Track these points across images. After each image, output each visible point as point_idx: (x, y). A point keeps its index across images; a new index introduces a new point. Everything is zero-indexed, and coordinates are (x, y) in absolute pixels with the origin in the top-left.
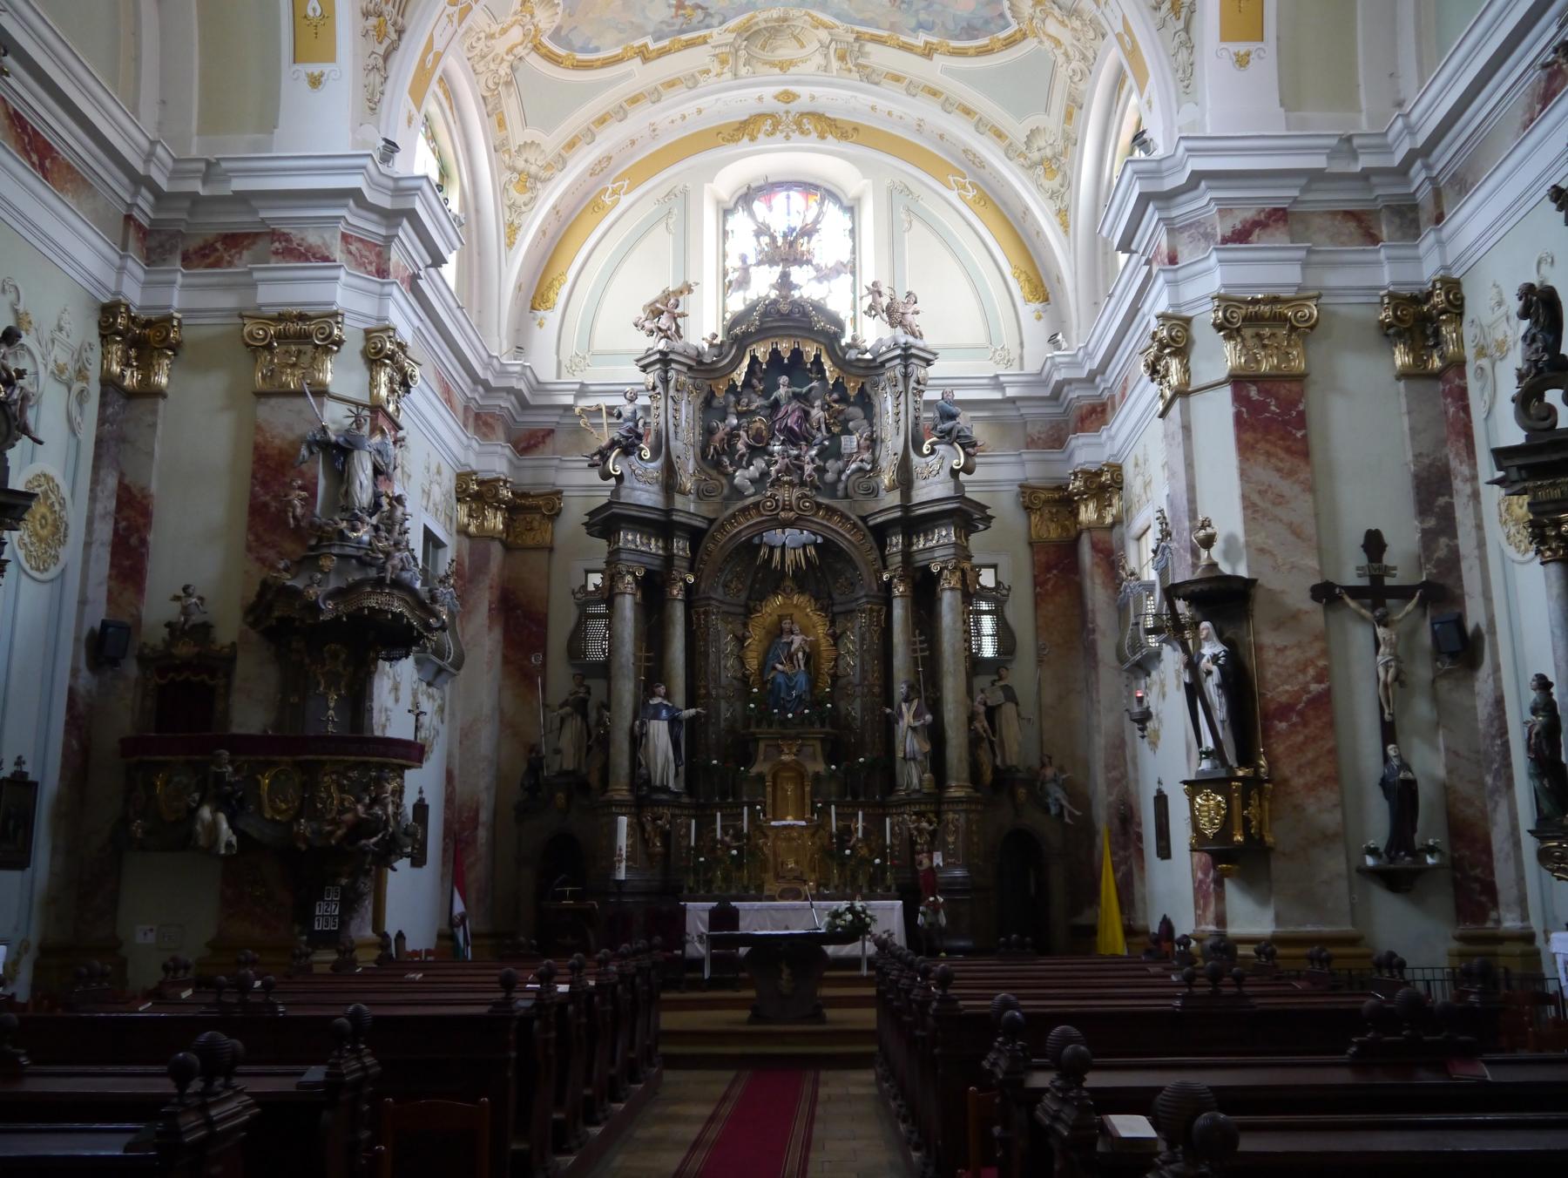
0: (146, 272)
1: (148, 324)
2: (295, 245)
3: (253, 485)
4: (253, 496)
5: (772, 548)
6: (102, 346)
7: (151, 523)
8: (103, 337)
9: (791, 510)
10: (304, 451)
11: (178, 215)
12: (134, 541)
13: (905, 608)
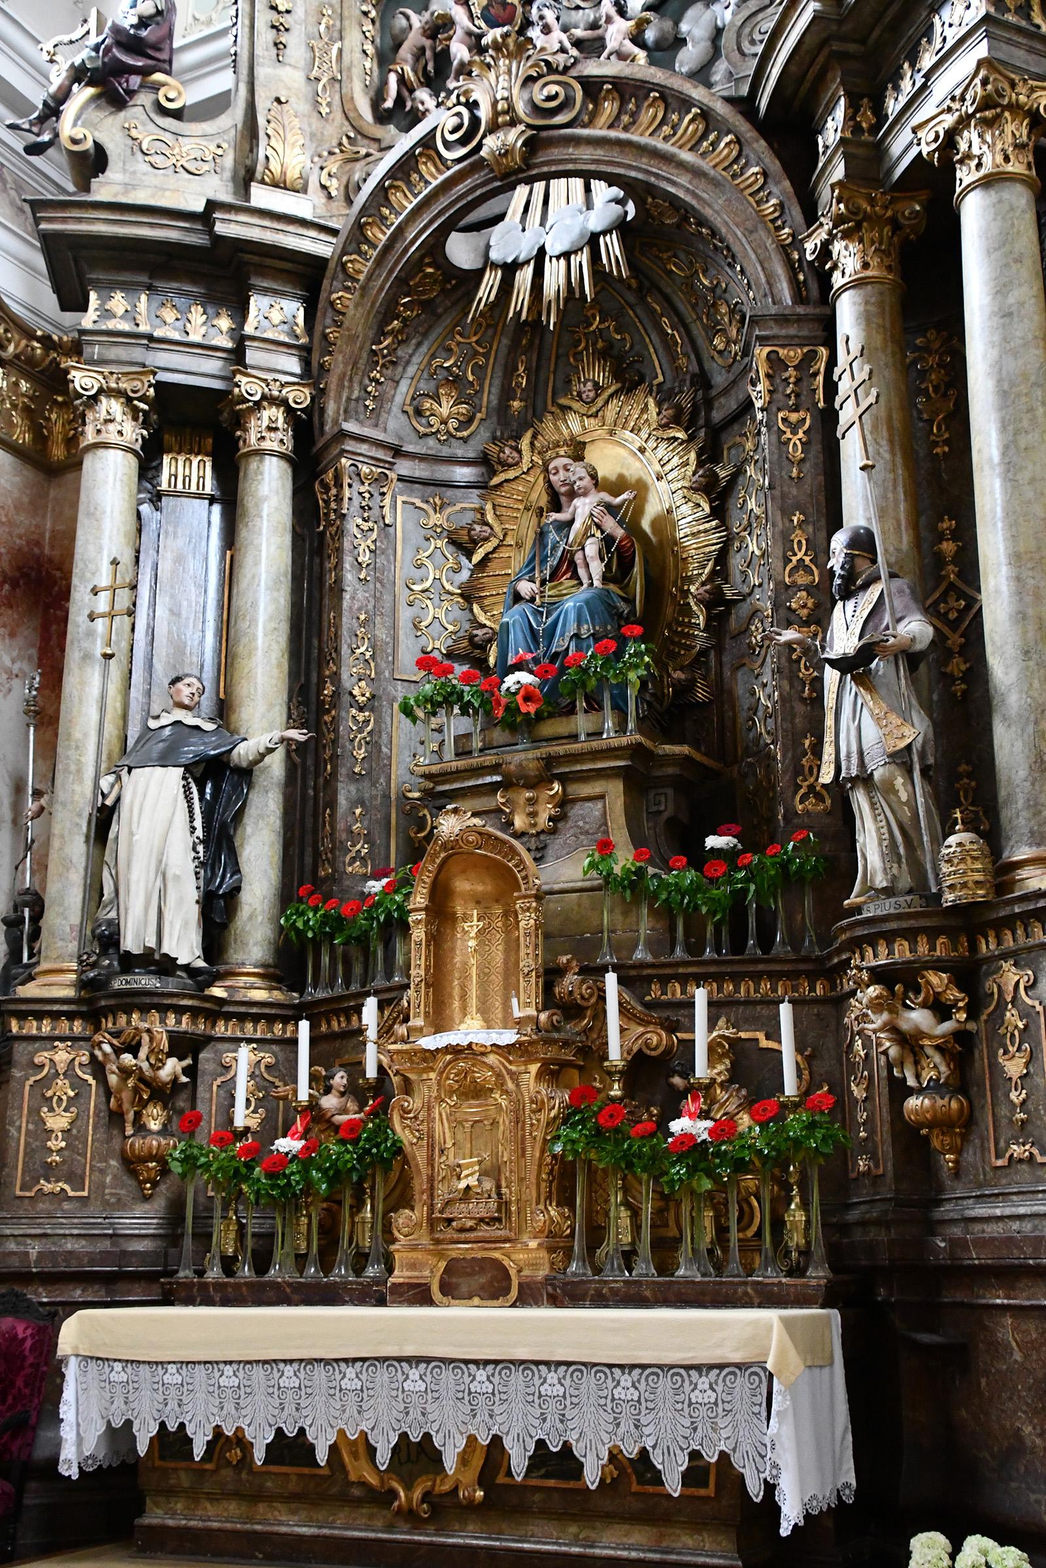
5: (510, 269)
9: (513, 123)
13: (867, 319)
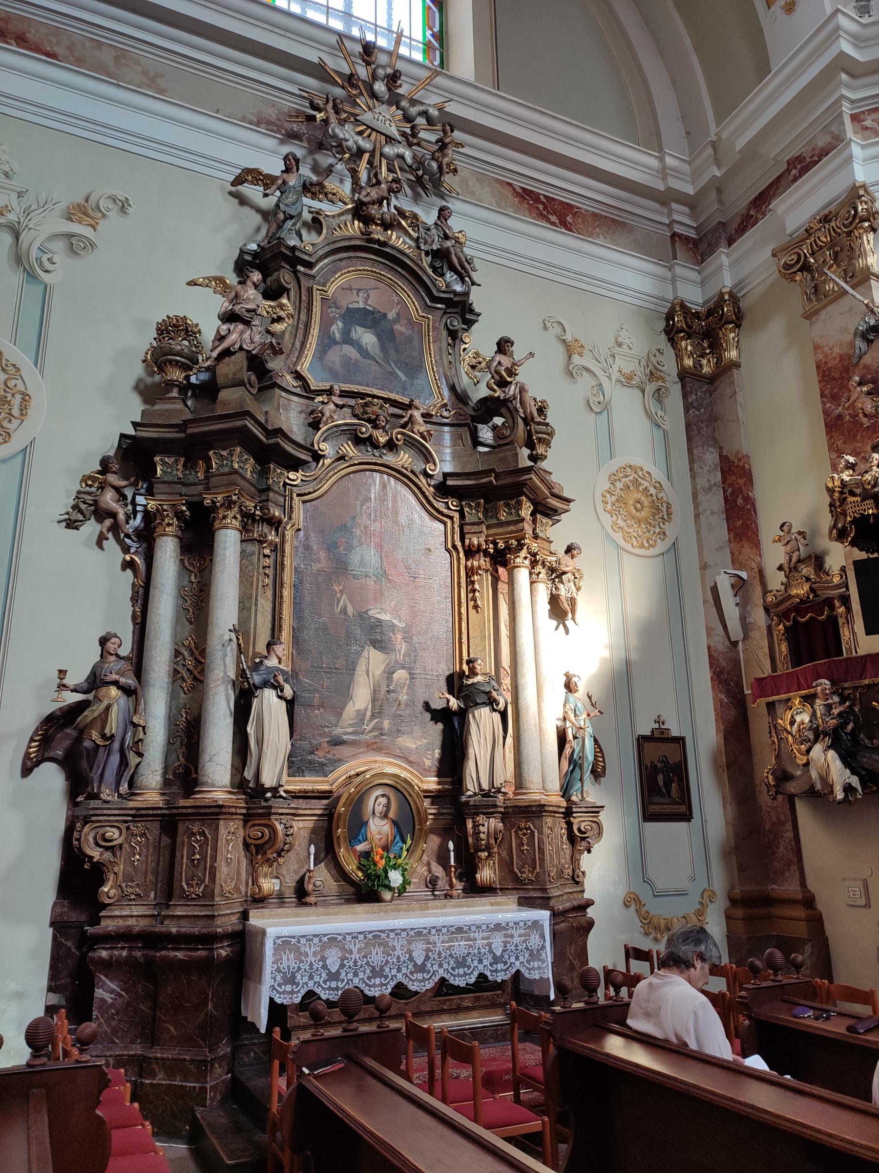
0: (699, 272)
1: (710, 312)
2: (808, 160)
3: (824, 404)
4: (826, 413)
6: (674, 348)
7: (751, 482)
8: (671, 340)
10: (860, 344)
11: (711, 209)
12: (740, 501)
